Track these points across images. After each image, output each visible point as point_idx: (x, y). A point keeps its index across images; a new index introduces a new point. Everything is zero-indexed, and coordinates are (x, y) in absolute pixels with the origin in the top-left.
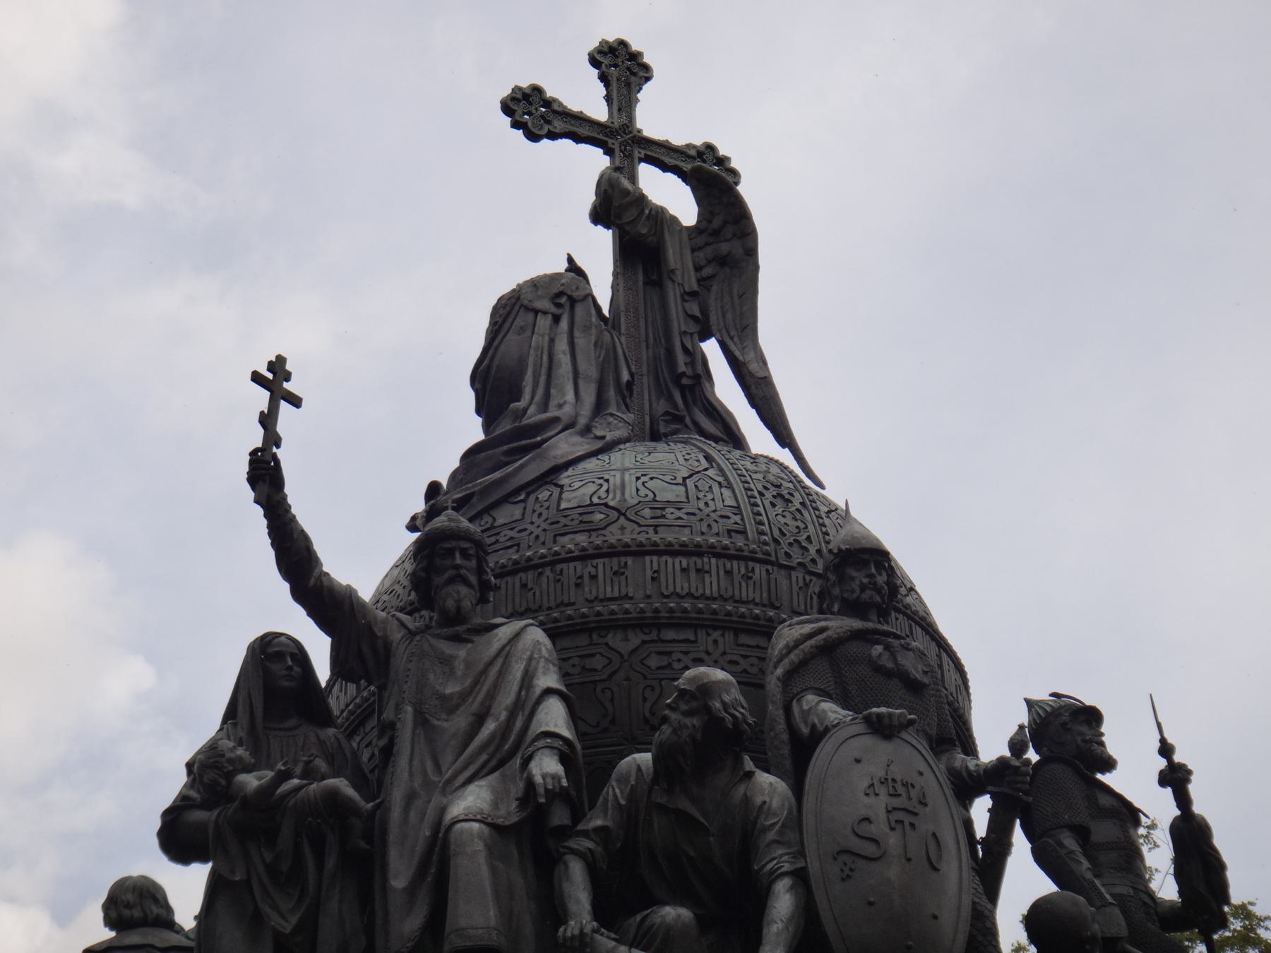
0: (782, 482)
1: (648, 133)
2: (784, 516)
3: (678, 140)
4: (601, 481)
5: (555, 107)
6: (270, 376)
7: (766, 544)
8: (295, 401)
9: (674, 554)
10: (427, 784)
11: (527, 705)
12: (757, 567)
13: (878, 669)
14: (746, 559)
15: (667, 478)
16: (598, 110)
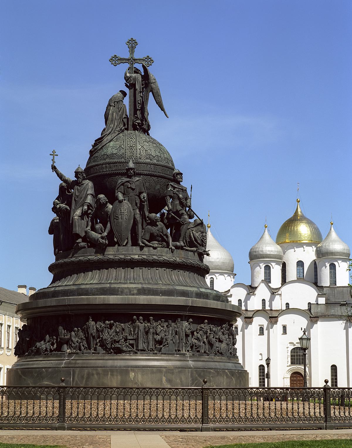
0: (133, 145)
1: (136, 58)
2: (130, 153)
3: (141, 58)
4: (107, 150)
5: (119, 58)
6: (53, 153)
7: (126, 160)
8: (57, 155)
9: (113, 164)
10: (75, 208)
11: (86, 197)
12: (124, 164)
13: (128, 187)
14: (123, 163)
15: (115, 149)
16: (127, 56)
